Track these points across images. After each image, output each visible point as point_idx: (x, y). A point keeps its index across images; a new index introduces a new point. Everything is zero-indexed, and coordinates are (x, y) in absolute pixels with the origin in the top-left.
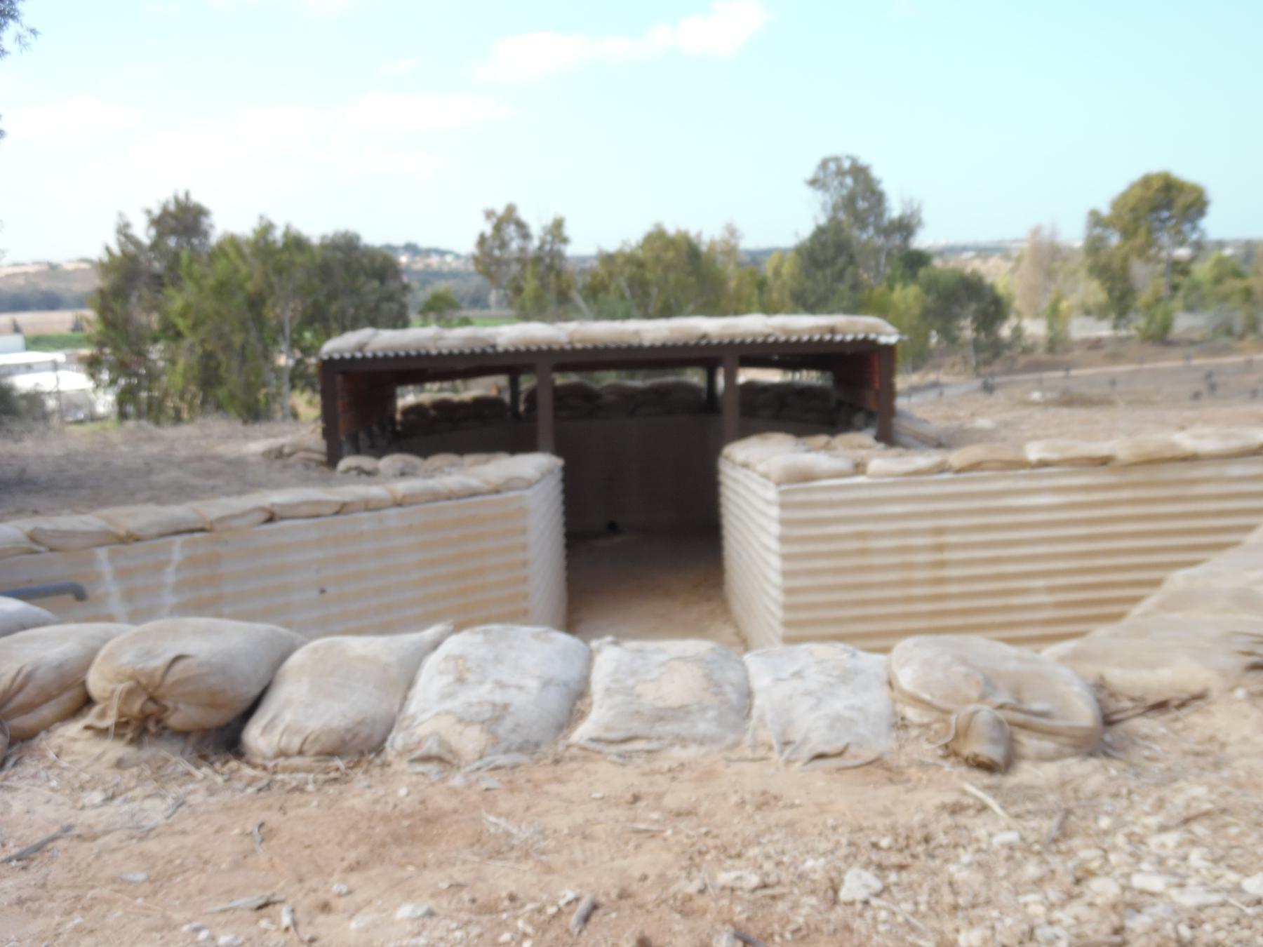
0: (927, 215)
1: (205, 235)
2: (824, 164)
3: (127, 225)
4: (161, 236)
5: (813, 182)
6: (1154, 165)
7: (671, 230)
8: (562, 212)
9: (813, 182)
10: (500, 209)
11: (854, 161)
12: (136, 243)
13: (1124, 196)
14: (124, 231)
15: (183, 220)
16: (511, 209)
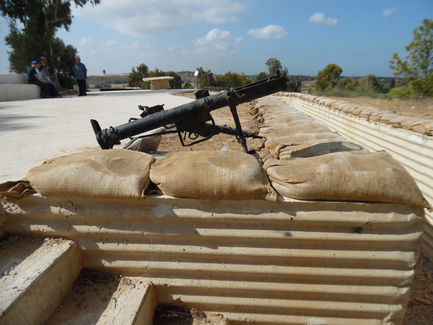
0: (289, 71)
1: (147, 71)
2: (269, 61)
3: (134, 69)
4: (139, 72)
5: (267, 64)
6: (332, 62)
7: (232, 73)
8: (210, 69)
9: (267, 64)
10: (199, 68)
11: (276, 60)
12: (136, 72)
13: (325, 68)
14: (133, 70)
15: (143, 69)
16: (201, 68)
